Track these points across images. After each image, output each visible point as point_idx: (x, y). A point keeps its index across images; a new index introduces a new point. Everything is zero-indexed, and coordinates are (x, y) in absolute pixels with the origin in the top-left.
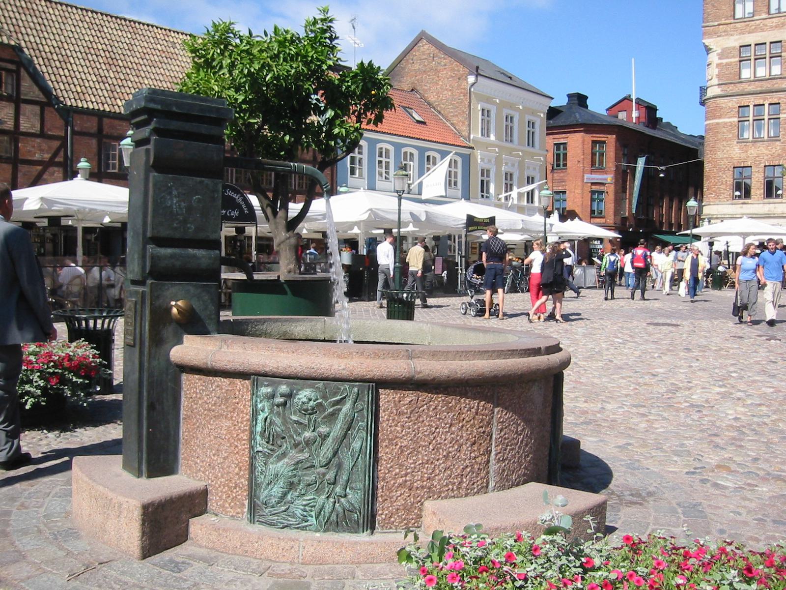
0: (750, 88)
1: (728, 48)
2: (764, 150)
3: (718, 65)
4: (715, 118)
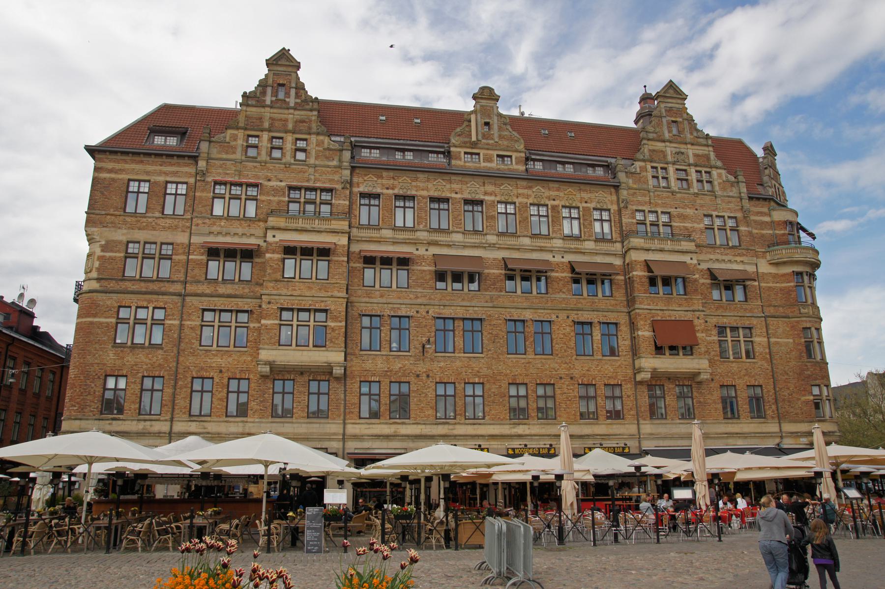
0: (132, 287)
1: (113, 241)
2: (143, 359)
3: (100, 258)
4: (89, 317)
